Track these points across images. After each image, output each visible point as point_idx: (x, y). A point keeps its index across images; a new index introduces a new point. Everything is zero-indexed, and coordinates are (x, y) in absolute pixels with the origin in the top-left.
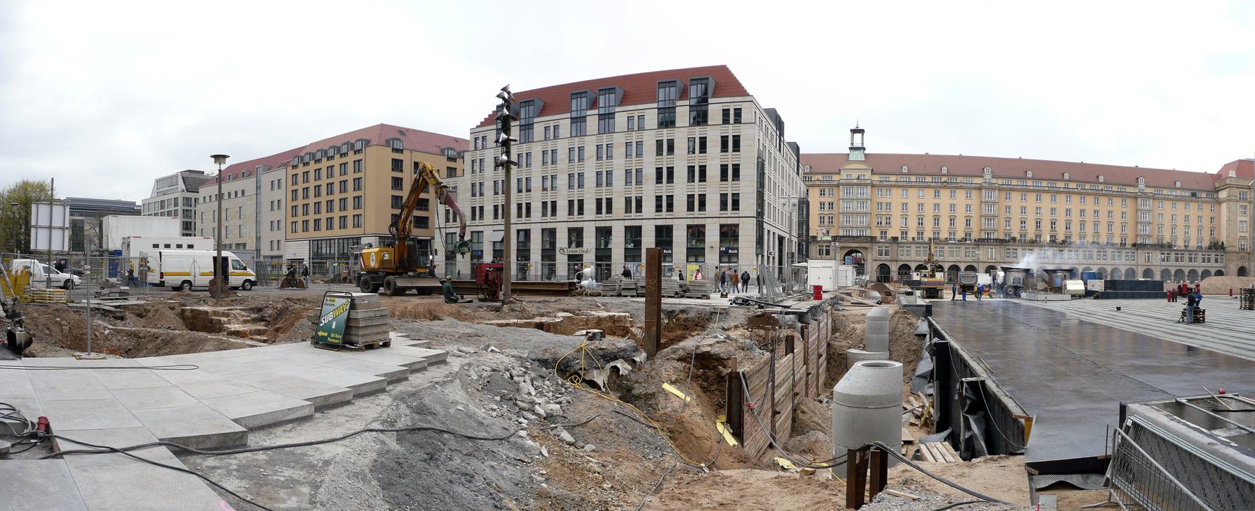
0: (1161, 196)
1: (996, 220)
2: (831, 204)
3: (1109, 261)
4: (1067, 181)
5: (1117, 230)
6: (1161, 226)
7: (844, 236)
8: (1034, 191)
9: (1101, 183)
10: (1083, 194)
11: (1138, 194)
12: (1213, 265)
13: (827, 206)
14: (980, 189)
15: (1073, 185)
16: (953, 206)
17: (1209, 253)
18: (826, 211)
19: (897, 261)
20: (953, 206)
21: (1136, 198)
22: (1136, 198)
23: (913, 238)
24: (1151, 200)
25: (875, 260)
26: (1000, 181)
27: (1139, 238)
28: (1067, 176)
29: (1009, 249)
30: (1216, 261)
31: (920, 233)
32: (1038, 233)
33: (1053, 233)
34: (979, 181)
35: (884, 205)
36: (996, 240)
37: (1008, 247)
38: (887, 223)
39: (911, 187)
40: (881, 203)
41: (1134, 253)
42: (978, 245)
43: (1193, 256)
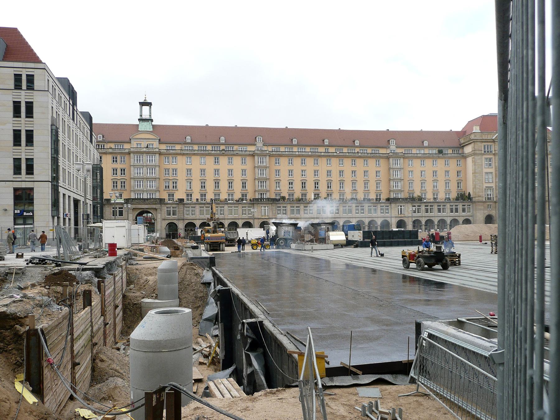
0: (410, 155)
1: (268, 182)
2: (123, 170)
3: (366, 214)
4: (327, 146)
5: (372, 187)
6: (411, 182)
7: (135, 199)
8: (299, 156)
9: (357, 147)
10: (341, 157)
11: (390, 155)
12: (461, 215)
13: (119, 172)
14: (253, 155)
15: (332, 150)
16: (230, 171)
17: (457, 204)
18: (119, 176)
19: (183, 220)
20: (230, 171)
21: (388, 158)
22: (388, 158)
23: (197, 200)
24: (402, 160)
25: (164, 220)
26: (270, 149)
27: (392, 194)
28: (327, 142)
29: (280, 207)
30: (464, 210)
31: (203, 195)
32: (304, 192)
33: (317, 192)
34: (251, 148)
35: (171, 171)
36: (268, 199)
37: (278, 205)
38: (173, 187)
39: (194, 154)
40: (168, 170)
41: (388, 207)
42: (253, 204)
43: (441, 207)
